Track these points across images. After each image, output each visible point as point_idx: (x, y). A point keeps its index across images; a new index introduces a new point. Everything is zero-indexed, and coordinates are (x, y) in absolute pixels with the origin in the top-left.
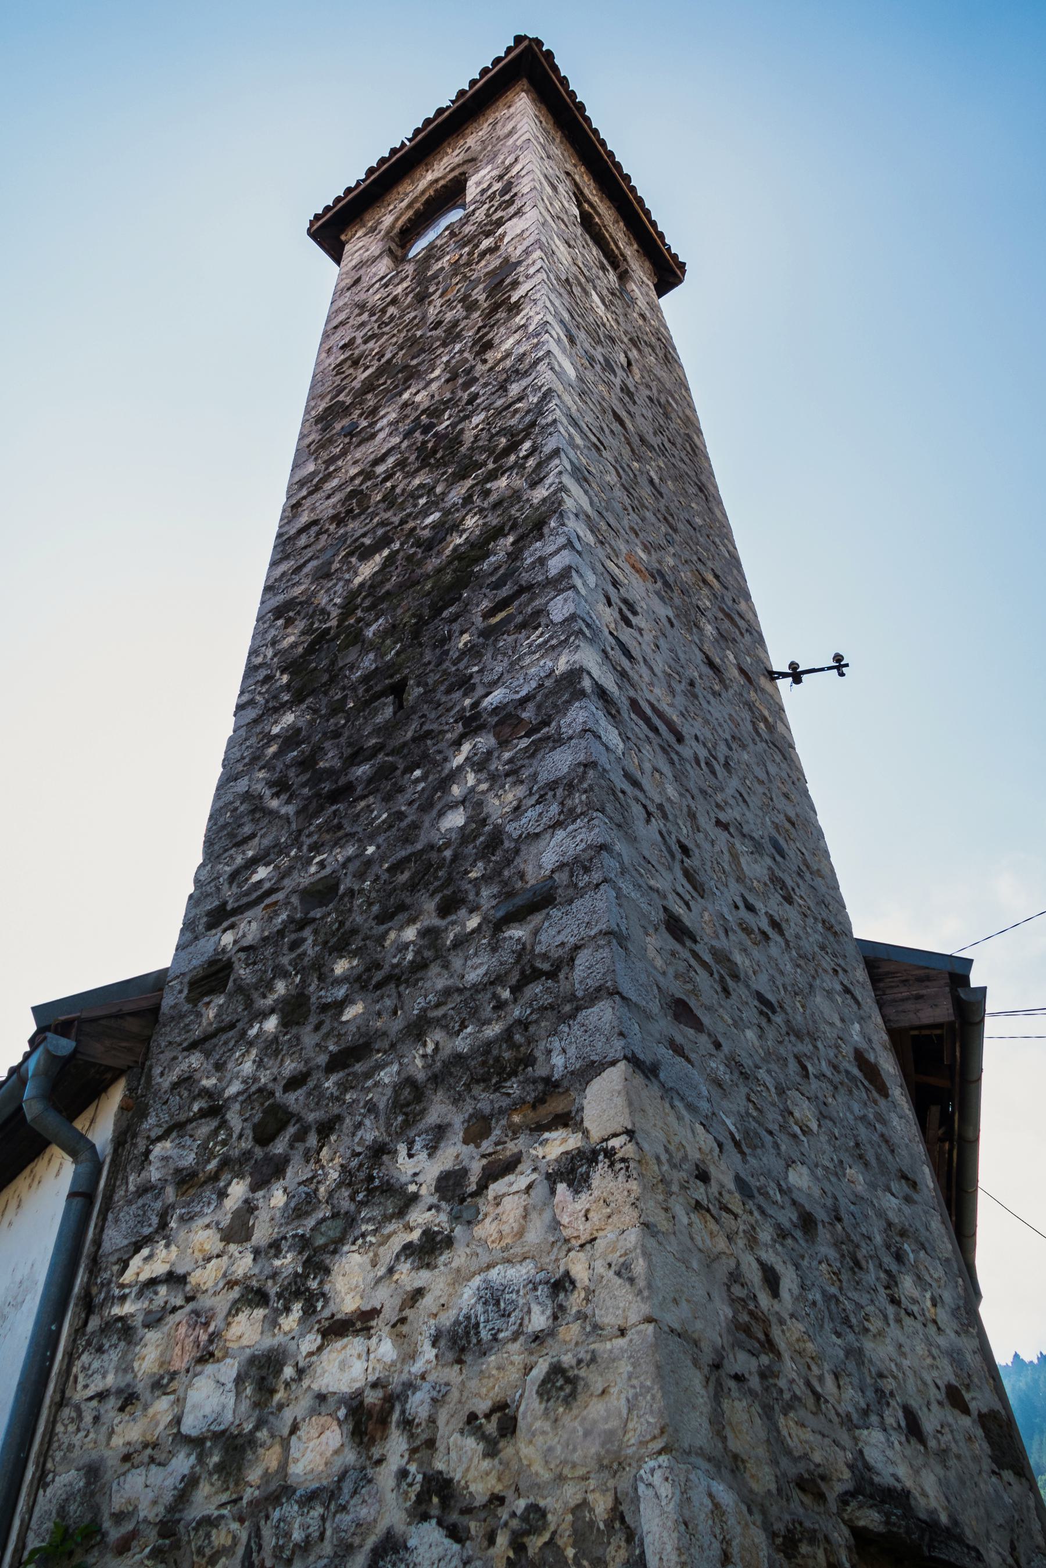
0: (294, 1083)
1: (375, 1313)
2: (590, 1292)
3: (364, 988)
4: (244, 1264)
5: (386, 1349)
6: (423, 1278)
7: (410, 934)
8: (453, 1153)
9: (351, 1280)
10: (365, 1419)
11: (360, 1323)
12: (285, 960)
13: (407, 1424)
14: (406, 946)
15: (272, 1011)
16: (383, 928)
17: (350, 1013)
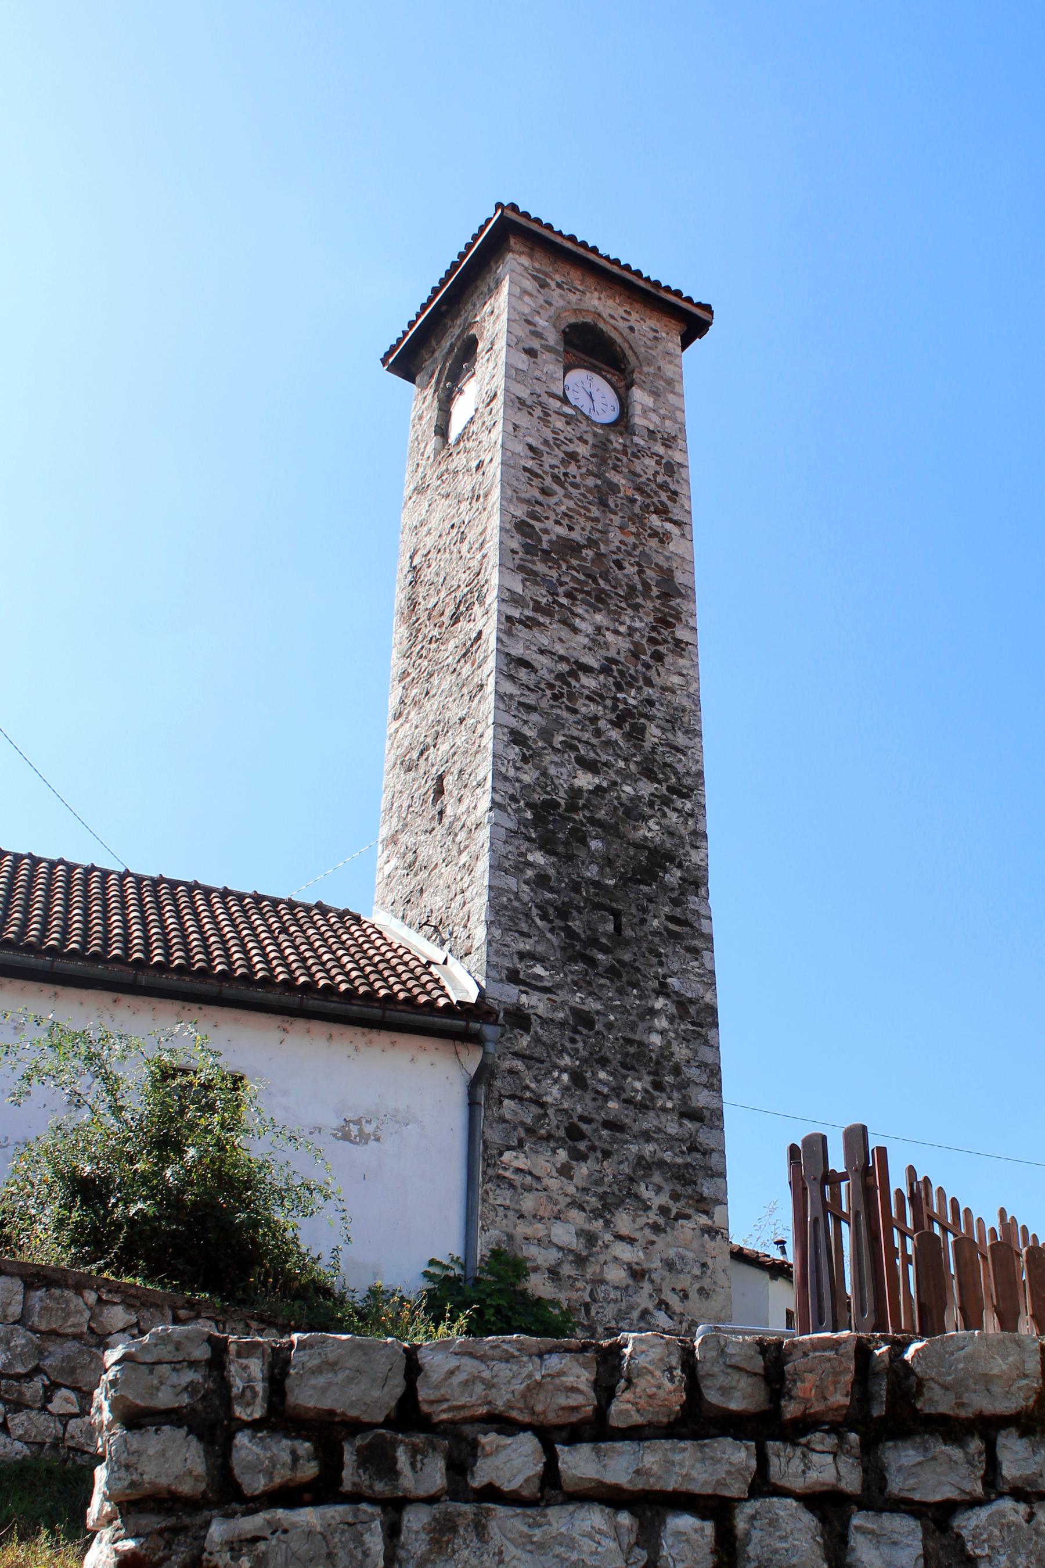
0: (581, 1118)
1: (635, 1240)
2: (713, 1272)
3: (618, 1096)
4: (571, 1190)
5: (641, 1254)
6: (654, 1238)
7: (638, 1085)
8: (663, 1199)
9: (623, 1222)
10: (637, 1274)
11: (631, 1241)
12: (568, 1045)
13: (652, 1281)
14: (637, 1091)
15: (565, 1071)
16: (624, 1071)
17: (611, 1104)
